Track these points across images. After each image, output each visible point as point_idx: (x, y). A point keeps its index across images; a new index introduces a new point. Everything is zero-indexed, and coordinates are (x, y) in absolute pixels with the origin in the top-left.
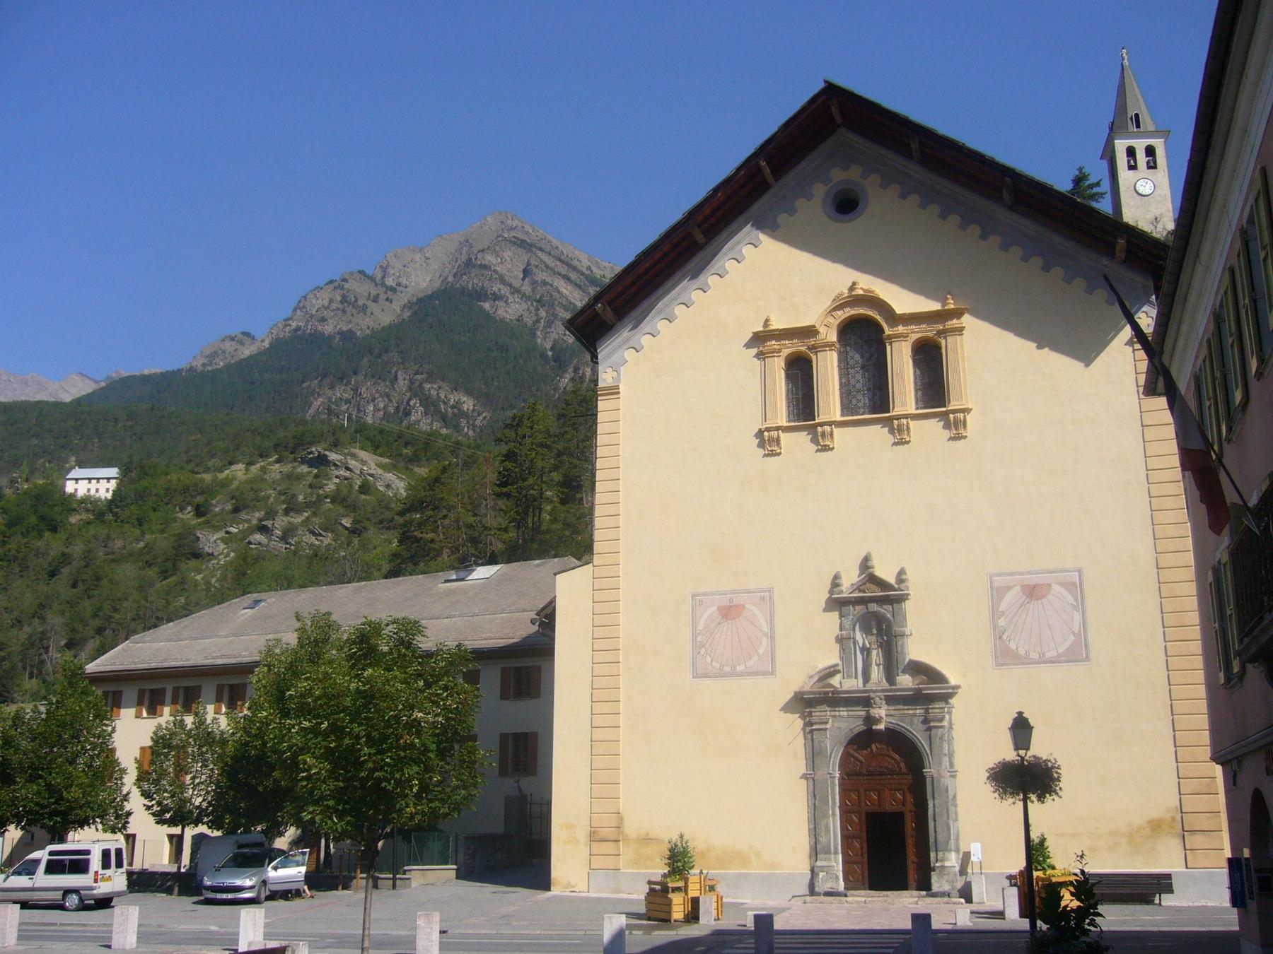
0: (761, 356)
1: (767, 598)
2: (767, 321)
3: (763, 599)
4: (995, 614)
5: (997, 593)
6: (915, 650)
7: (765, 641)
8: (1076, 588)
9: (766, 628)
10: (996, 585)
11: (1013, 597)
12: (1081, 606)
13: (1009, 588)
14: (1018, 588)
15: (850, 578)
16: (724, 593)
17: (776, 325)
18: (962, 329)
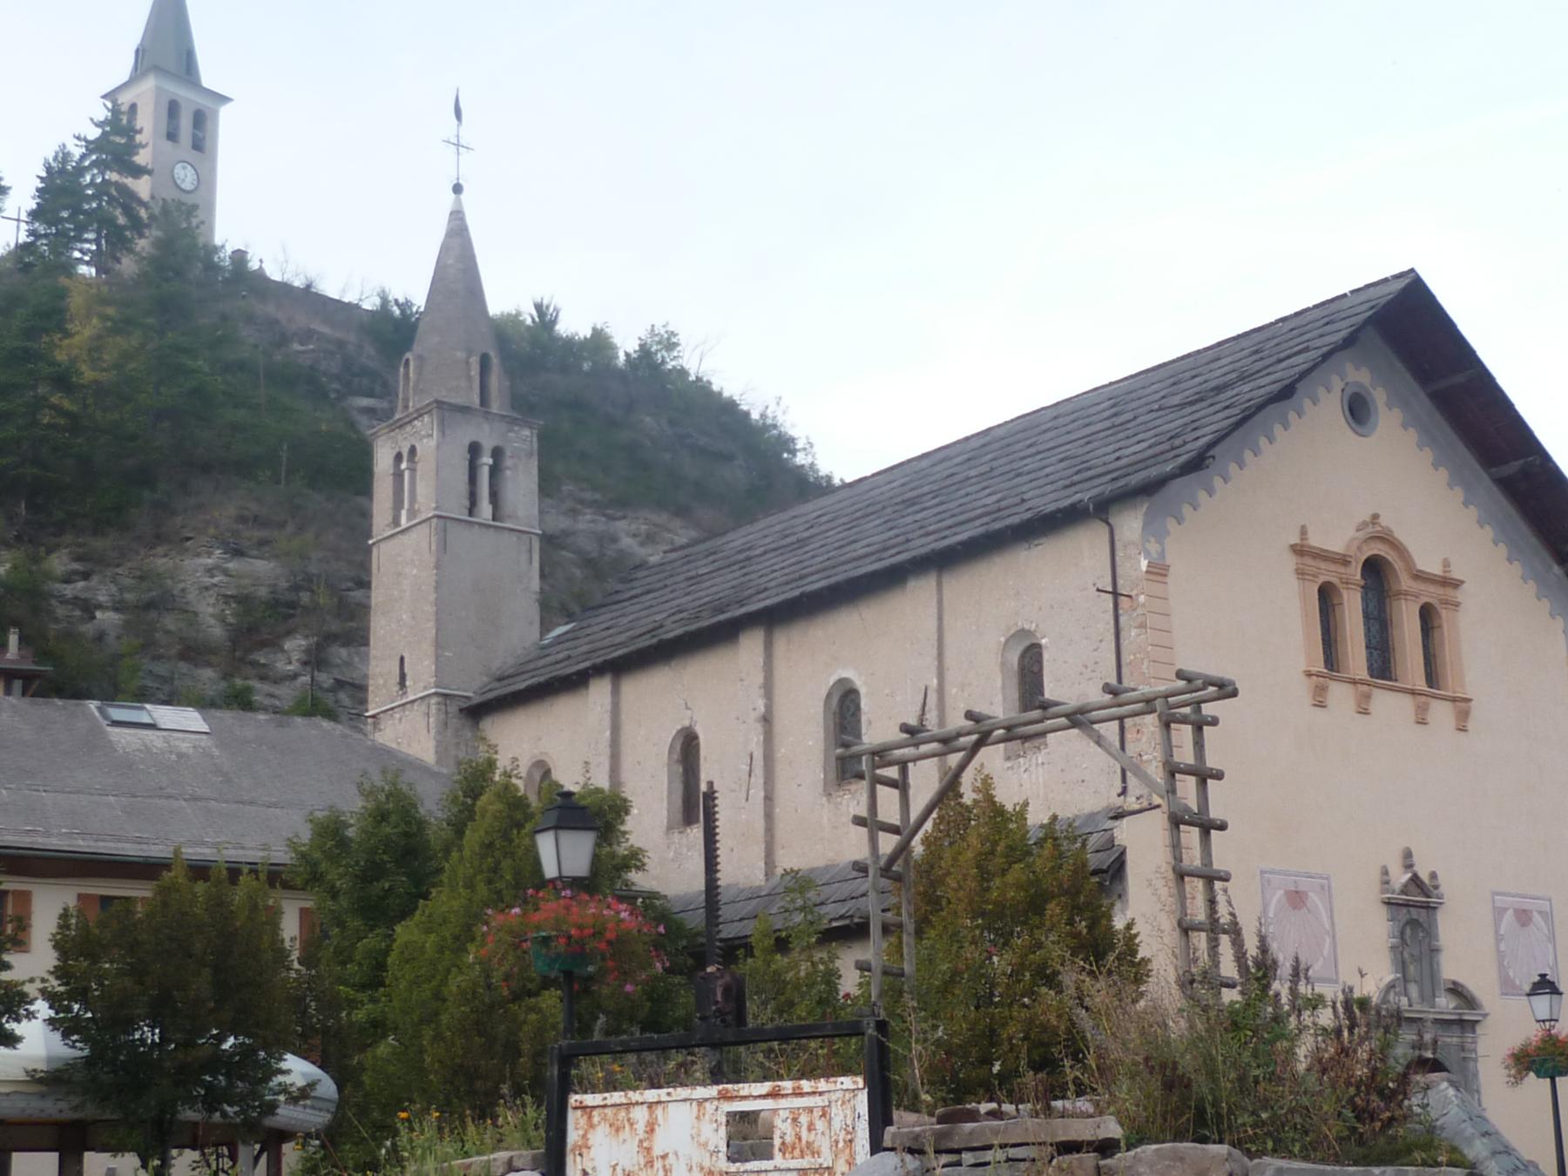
0: (1301, 573)
1: (1326, 890)
2: (1303, 532)
3: (1322, 887)
4: (1499, 938)
5: (1499, 912)
6: (1451, 968)
7: (1328, 940)
8: (1548, 916)
9: (1327, 926)
10: (1498, 904)
11: (1509, 916)
12: (1552, 938)
13: (1505, 910)
14: (1510, 912)
15: (1400, 878)
16: (1287, 873)
17: (1315, 541)
18: (1457, 605)
